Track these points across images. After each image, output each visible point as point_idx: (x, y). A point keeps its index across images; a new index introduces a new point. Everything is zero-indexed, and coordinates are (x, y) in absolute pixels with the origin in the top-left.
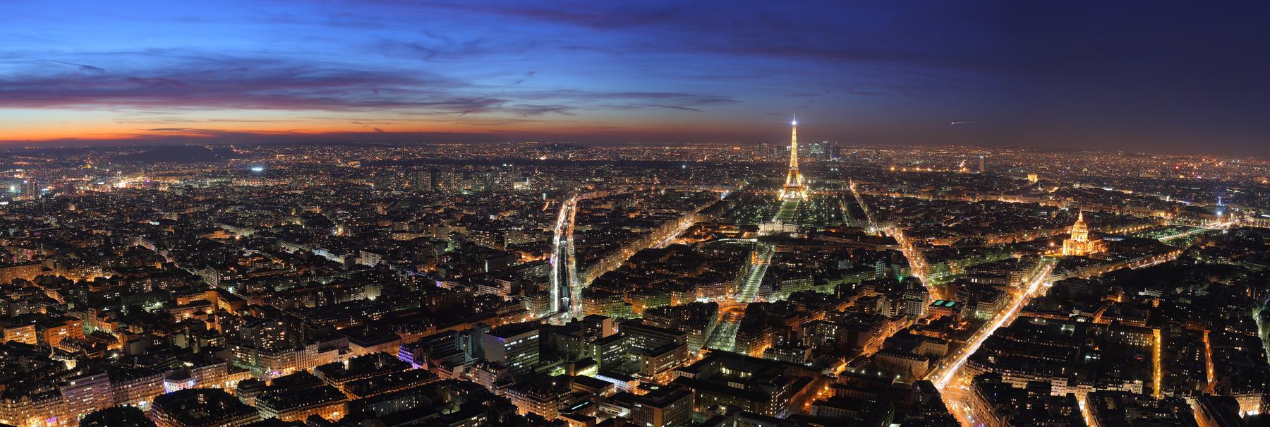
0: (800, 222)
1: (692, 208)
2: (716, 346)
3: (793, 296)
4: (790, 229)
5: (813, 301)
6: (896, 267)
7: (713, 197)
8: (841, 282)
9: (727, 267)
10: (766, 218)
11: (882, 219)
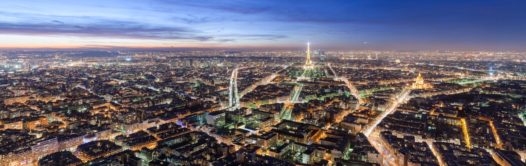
0: (311, 76)
3: (310, 101)
4: (308, 79)
5: (317, 103)
6: (346, 92)
9: (287, 91)
10: (300, 75)
11: (340, 75)
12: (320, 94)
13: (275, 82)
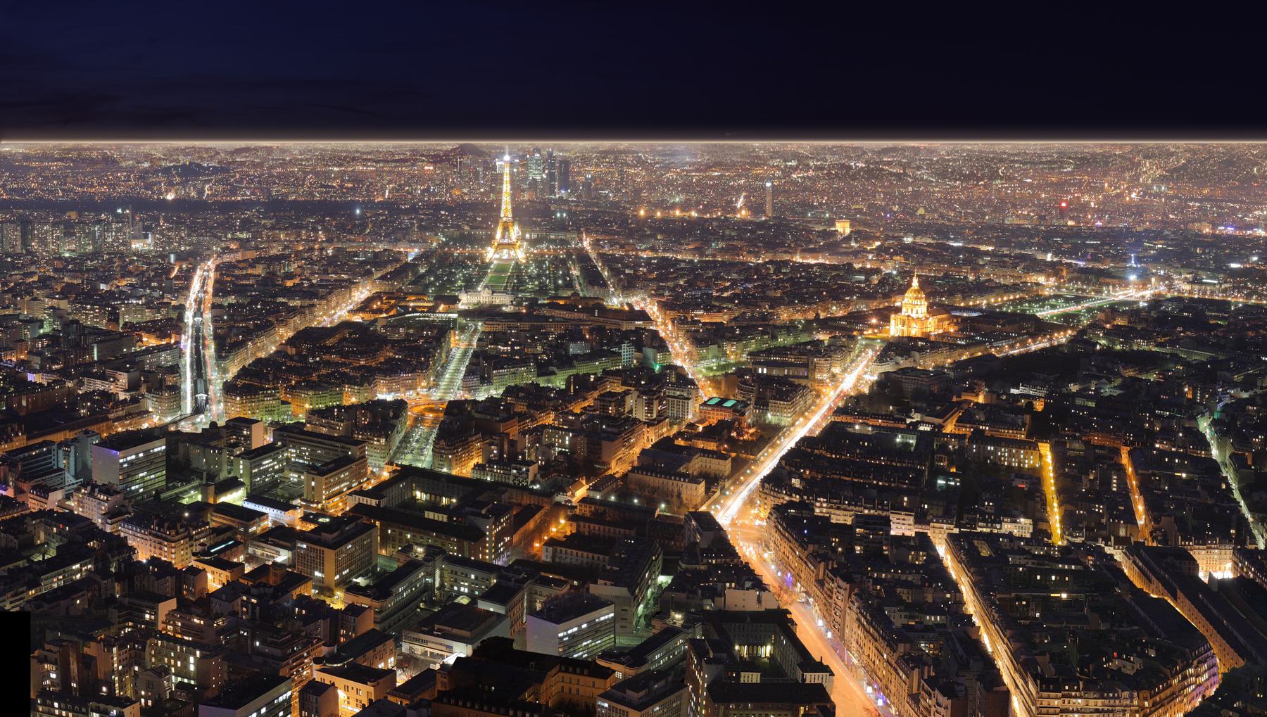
0: (516, 290)
1: (368, 274)
2: (406, 460)
3: (509, 391)
4: (505, 301)
5: (536, 398)
6: (649, 352)
7: (396, 258)
8: (573, 372)
9: (417, 351)
11: (628, 285)
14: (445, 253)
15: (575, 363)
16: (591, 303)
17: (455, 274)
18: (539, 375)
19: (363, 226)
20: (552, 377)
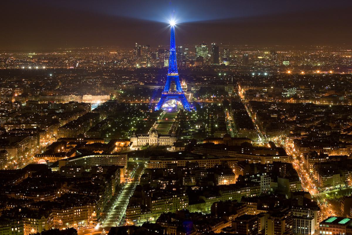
0: (178, 133)
1: (55, 123)
6: (283, 181)
10: (142, 131)
11: (272, 127)
12: (199, 192)
13: (52, 159)
14: (123, 104)
15: (221, 192)
16: (240, 143)
17: (130, 121)
18: (190, 204)
19: (54, 83)
20: (202, 205)
